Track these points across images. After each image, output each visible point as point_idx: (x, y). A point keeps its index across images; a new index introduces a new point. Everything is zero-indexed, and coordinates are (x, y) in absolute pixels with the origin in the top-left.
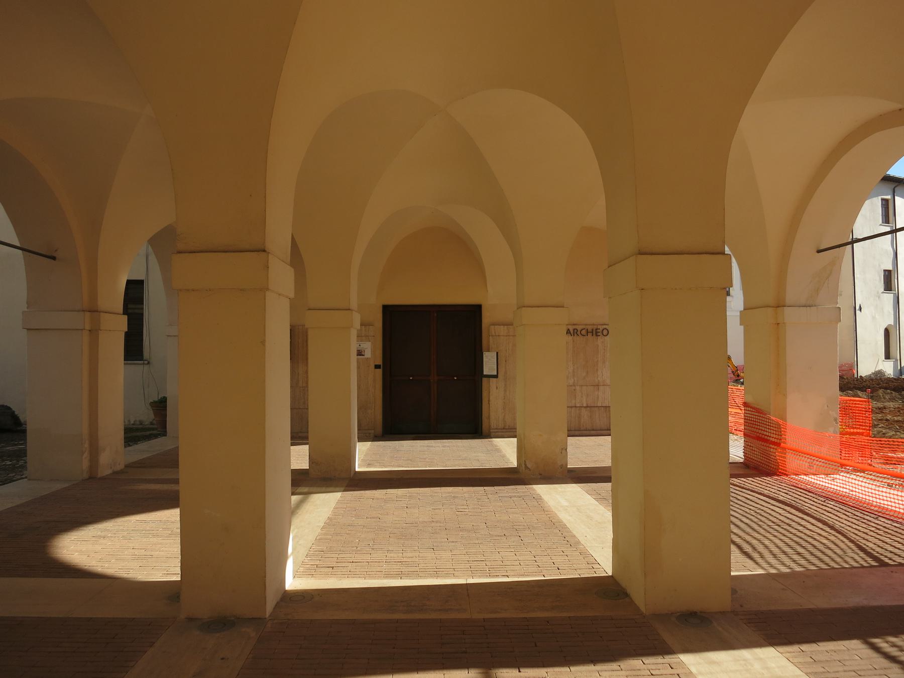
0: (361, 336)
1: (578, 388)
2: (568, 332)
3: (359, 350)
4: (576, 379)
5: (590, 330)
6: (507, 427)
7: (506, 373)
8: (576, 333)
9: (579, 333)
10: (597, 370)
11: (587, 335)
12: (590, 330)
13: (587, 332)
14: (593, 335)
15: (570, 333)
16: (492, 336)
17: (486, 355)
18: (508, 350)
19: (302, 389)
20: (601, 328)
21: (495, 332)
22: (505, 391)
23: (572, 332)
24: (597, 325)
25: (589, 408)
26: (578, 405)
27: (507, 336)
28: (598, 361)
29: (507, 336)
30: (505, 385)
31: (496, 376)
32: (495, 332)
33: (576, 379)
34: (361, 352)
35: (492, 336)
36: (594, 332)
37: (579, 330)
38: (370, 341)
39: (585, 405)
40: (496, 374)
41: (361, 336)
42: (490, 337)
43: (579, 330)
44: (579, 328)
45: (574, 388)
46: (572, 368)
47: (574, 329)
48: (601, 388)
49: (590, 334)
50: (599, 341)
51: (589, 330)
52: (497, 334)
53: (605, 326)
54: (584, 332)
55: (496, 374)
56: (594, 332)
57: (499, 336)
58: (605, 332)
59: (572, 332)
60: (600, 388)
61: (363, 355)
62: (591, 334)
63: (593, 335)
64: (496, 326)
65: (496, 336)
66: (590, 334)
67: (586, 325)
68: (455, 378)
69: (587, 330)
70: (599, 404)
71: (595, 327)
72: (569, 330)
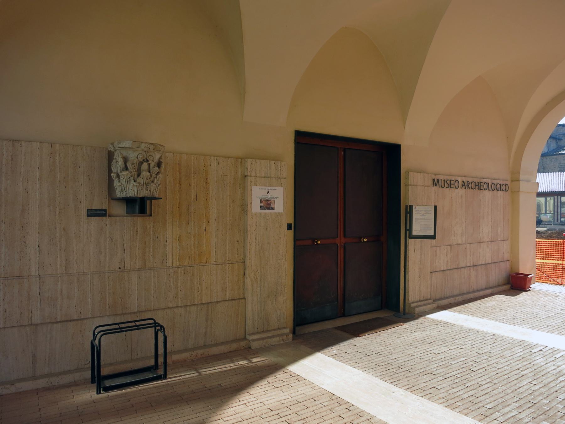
0: (270, 177)
3: (268, 200)
6: (422, 299)
10: (480, 226)
16: (411, 185)
17: (417, 209)
19: (171, 270)
22: (421, 254)
25: (475, 267)
26: (468, 265)
27: (422, 186)
28: (480, 216)
29: (422, 186)
30: (421, 247)
31: (433, 237)
34: (270, 204)
38: (282, 186)
39: (472, 265)
40: (433, 234)
41: (270, 177)
52: (415, 184)
55: (433, 234)
57: (416, 185)
61: (273, 209)
64: (415, 173)
68: (366, 240)
70: (480, 263)
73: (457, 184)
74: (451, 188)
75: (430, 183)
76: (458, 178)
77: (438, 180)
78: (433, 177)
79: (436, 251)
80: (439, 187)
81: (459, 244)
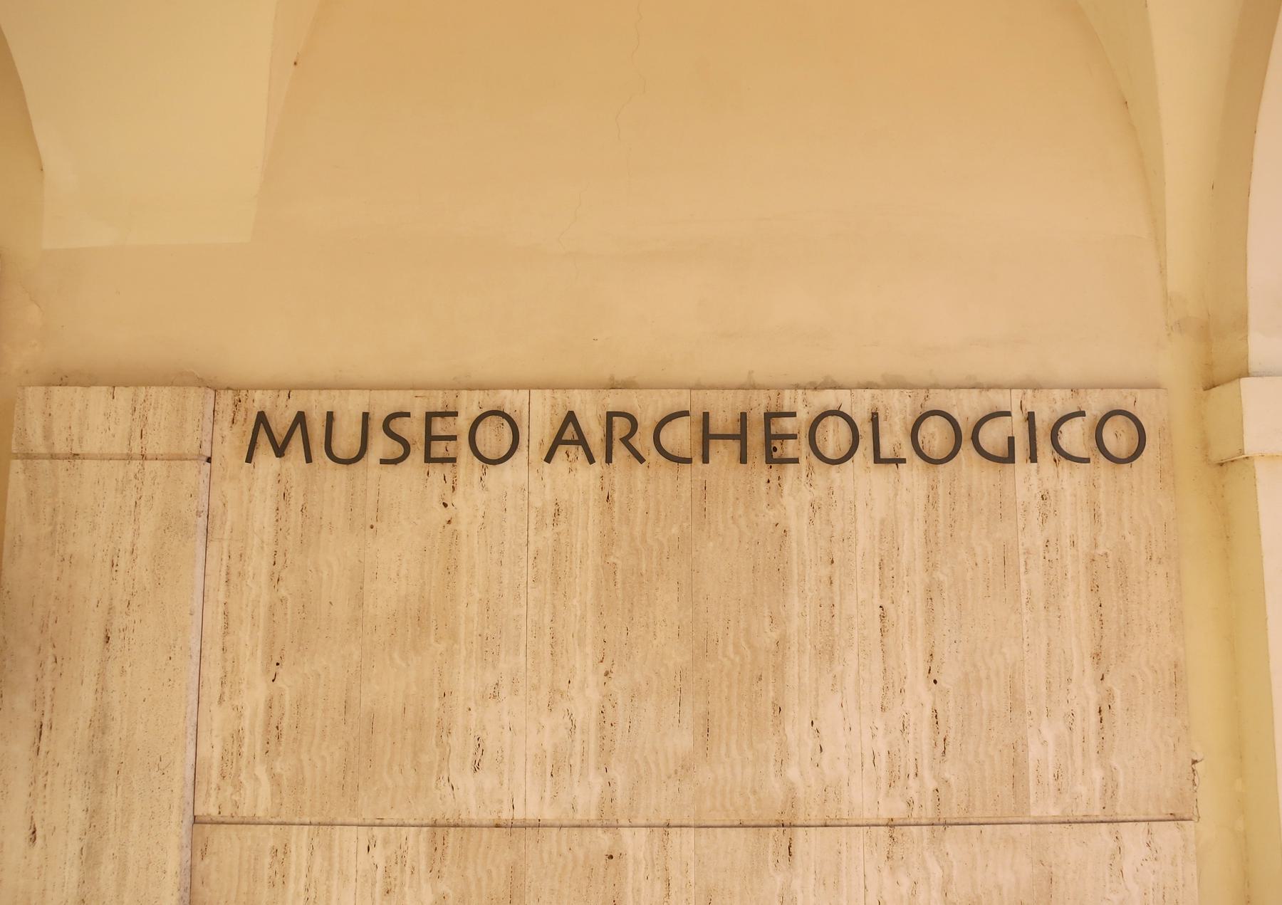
1: (635, 843)
2: (570, 433)
4: (619, 775)
5: (723, 421)
7: (100, 724)
8: (625, 441)
9: (643, 440)
11: (706, 460)
12: (723, 421)
13: (707, 437)
14: (743, 460)
15: (581, 441)
18: (123, 563)
20: (805, 407)
21: (47, 434)
22: (89, 857)
23: (595, 436)
24: (780, 389)
28: (781, 644)
29: (129, 458)
32: (47, 434)
33: (619, 775)
35: (28, 456)
36: (756, 437)
37: (647, 423)
42: (17, 465)
43: (647, 423)
44: (649, 408)
45: (604, 840)
46: (593, 695)
47: (610, 415)
48: (809, 843)
49: (723, 453)
50: (787, 500)
51: (717, 426)
52: (61, 448)
53: (829, 399)
54: (680, 436)
56: (756, 437)
58: (834, 437)
59: (595, 436)
60: (798, 849)
62: (735, 445)
63: (743, 460)
65: (53, 457)
66: (723, 453)
67: (698, 387)
69: (706, 416)
71: (759, 404)
72: (571, 418)
73: (493, 438)
74: (429, 459)
75: (231, 441)
76: (511, 400)
77: (301, 418)
78: (261, 401)
79: (281, 853)
80: (309, 459)
81: (539, 825)
